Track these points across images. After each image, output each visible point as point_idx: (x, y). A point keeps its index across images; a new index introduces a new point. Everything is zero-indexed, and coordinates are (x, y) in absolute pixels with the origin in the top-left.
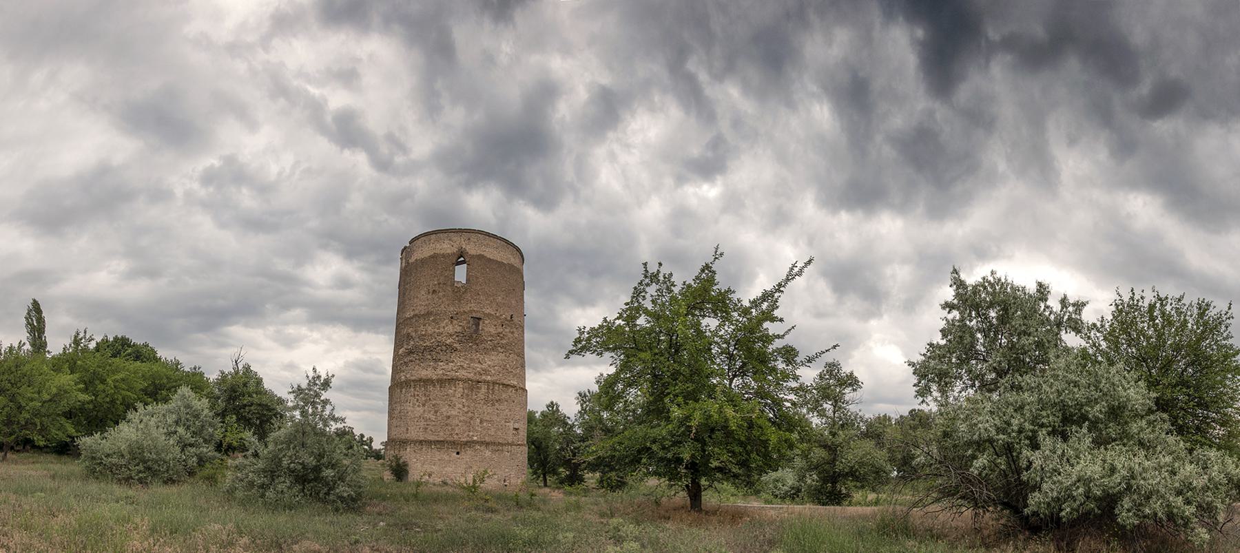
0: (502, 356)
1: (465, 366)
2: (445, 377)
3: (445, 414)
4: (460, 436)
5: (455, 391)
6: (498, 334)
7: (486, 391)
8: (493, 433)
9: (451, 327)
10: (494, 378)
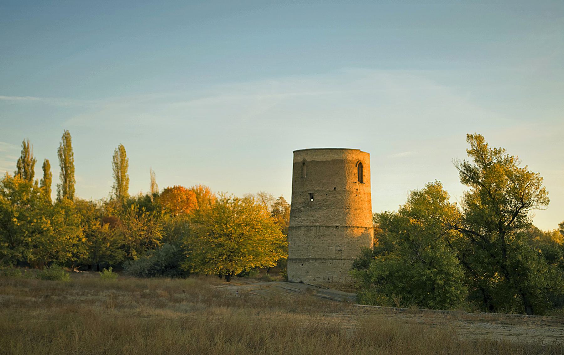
0: (325, 211)
1: (306, 219)
2: (298, 226)
4: (304, 256)
5: (301, 232)
7: (315, 231)
8: (320, 254)
10: (321, 224)
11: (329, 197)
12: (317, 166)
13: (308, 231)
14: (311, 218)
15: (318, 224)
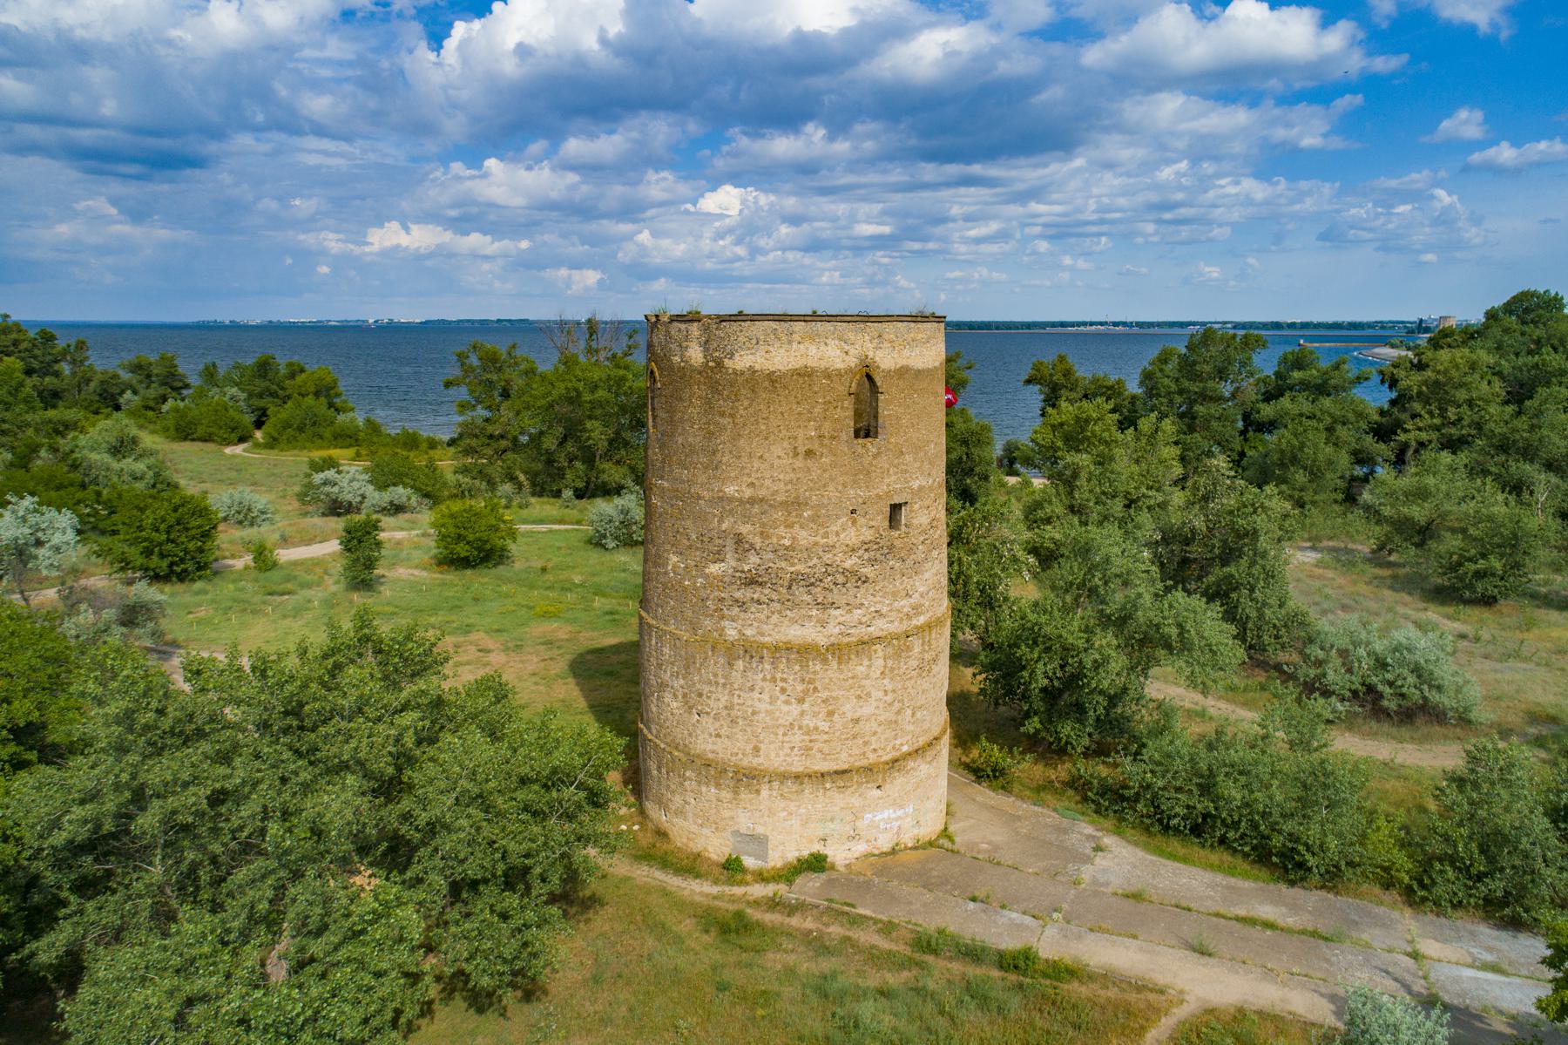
1: (885, 610)
2: (846, 640)
3: (849, 716)
5: (870, 666)
9: (852, 532)
13: (897, 655)
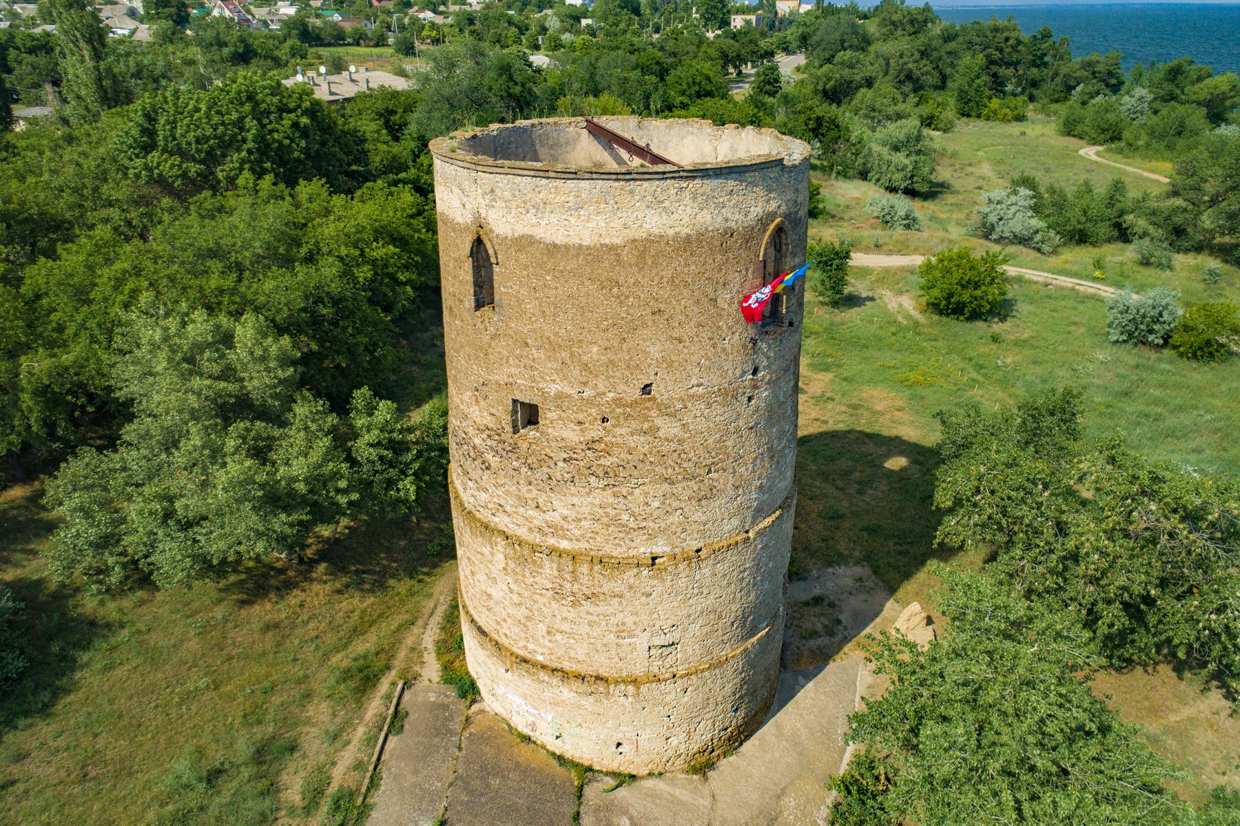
6: (590, 445)
7: (556, 573)
11: (618, 431)
12: (548, 272)
14: (531, 512)
15: (564, 545)
